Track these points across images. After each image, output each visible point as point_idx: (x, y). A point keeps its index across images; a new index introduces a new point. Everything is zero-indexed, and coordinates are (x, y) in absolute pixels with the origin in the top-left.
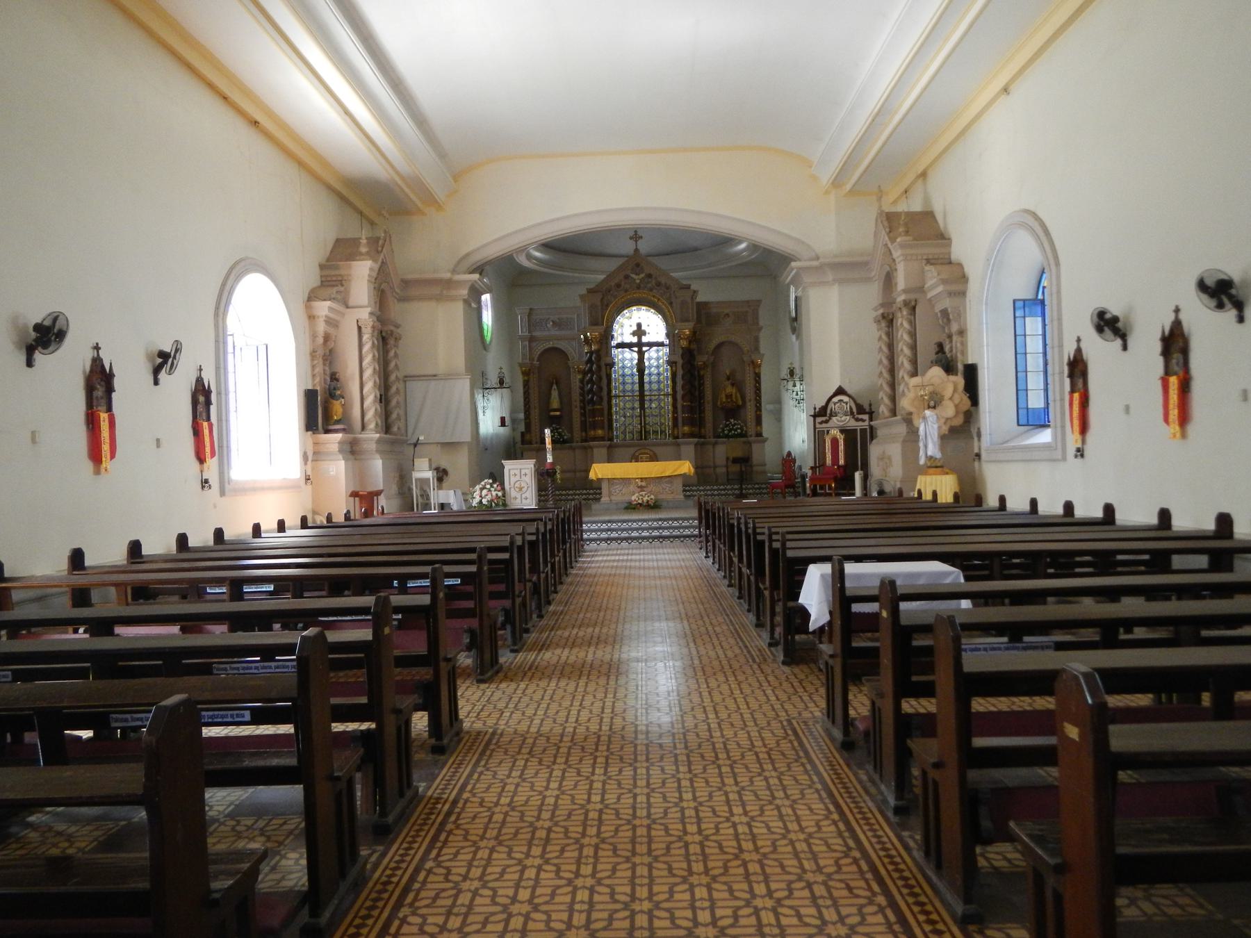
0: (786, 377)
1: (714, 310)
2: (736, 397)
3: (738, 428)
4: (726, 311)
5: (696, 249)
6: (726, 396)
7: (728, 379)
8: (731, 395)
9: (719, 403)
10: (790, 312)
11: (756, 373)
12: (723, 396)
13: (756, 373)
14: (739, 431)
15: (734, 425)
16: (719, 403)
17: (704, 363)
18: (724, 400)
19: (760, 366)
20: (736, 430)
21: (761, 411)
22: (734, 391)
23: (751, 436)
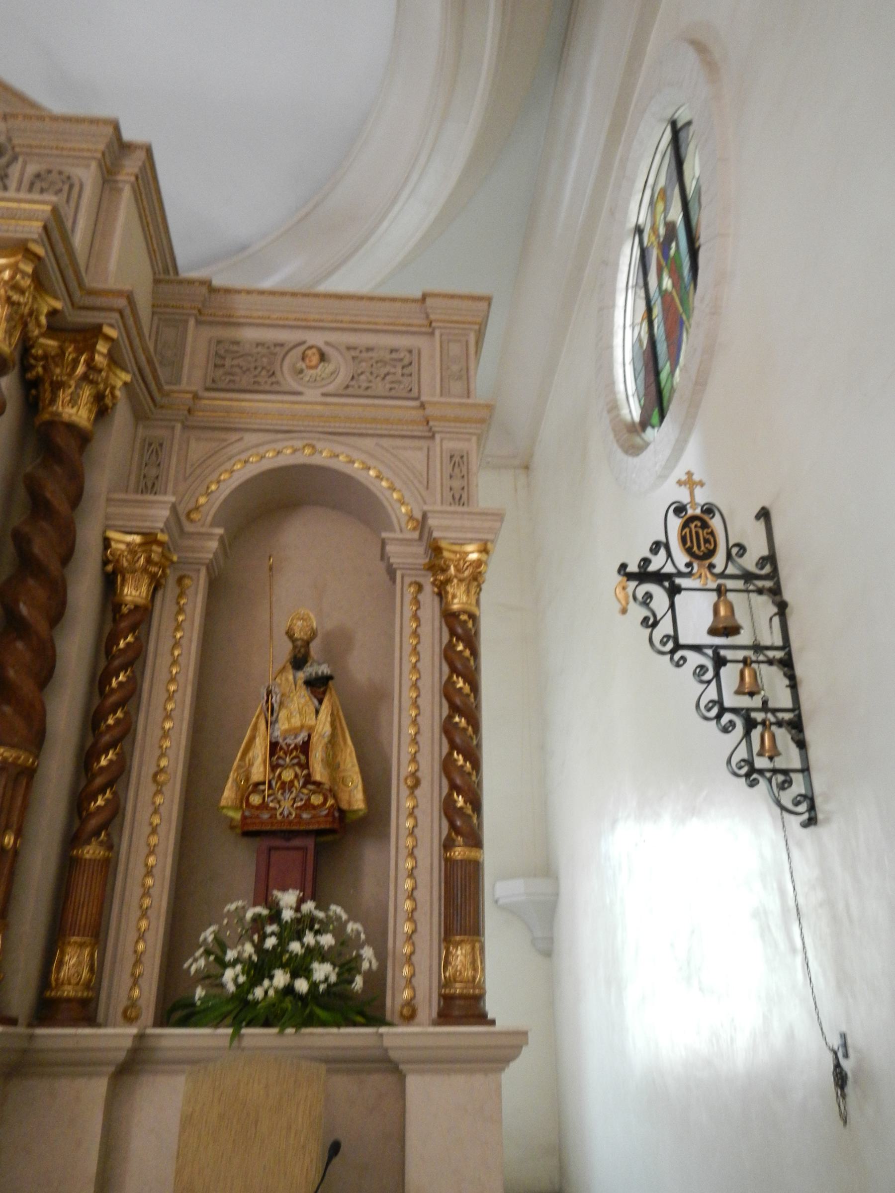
0: (657, 563)
1: (250, 334)
2: (332, 764)
3: (315, 953)
4: (317, 339)
5: (244, 248)
6: (274, 747)
7: (299, 662)
8: (305, 748)
9: (228, 794)
10: (613, 407)
11: (450, 617)
12: (260, 751)
13: (450, 617)
14: (322, 971)
15: (297, 929)
16: (228, 794)
17: (150, 539)
18: (258, 772)
19: (476, 579)
20: (299, 968)
21: (475, 841)
22: (323, 726)
23: (409, 1016)
